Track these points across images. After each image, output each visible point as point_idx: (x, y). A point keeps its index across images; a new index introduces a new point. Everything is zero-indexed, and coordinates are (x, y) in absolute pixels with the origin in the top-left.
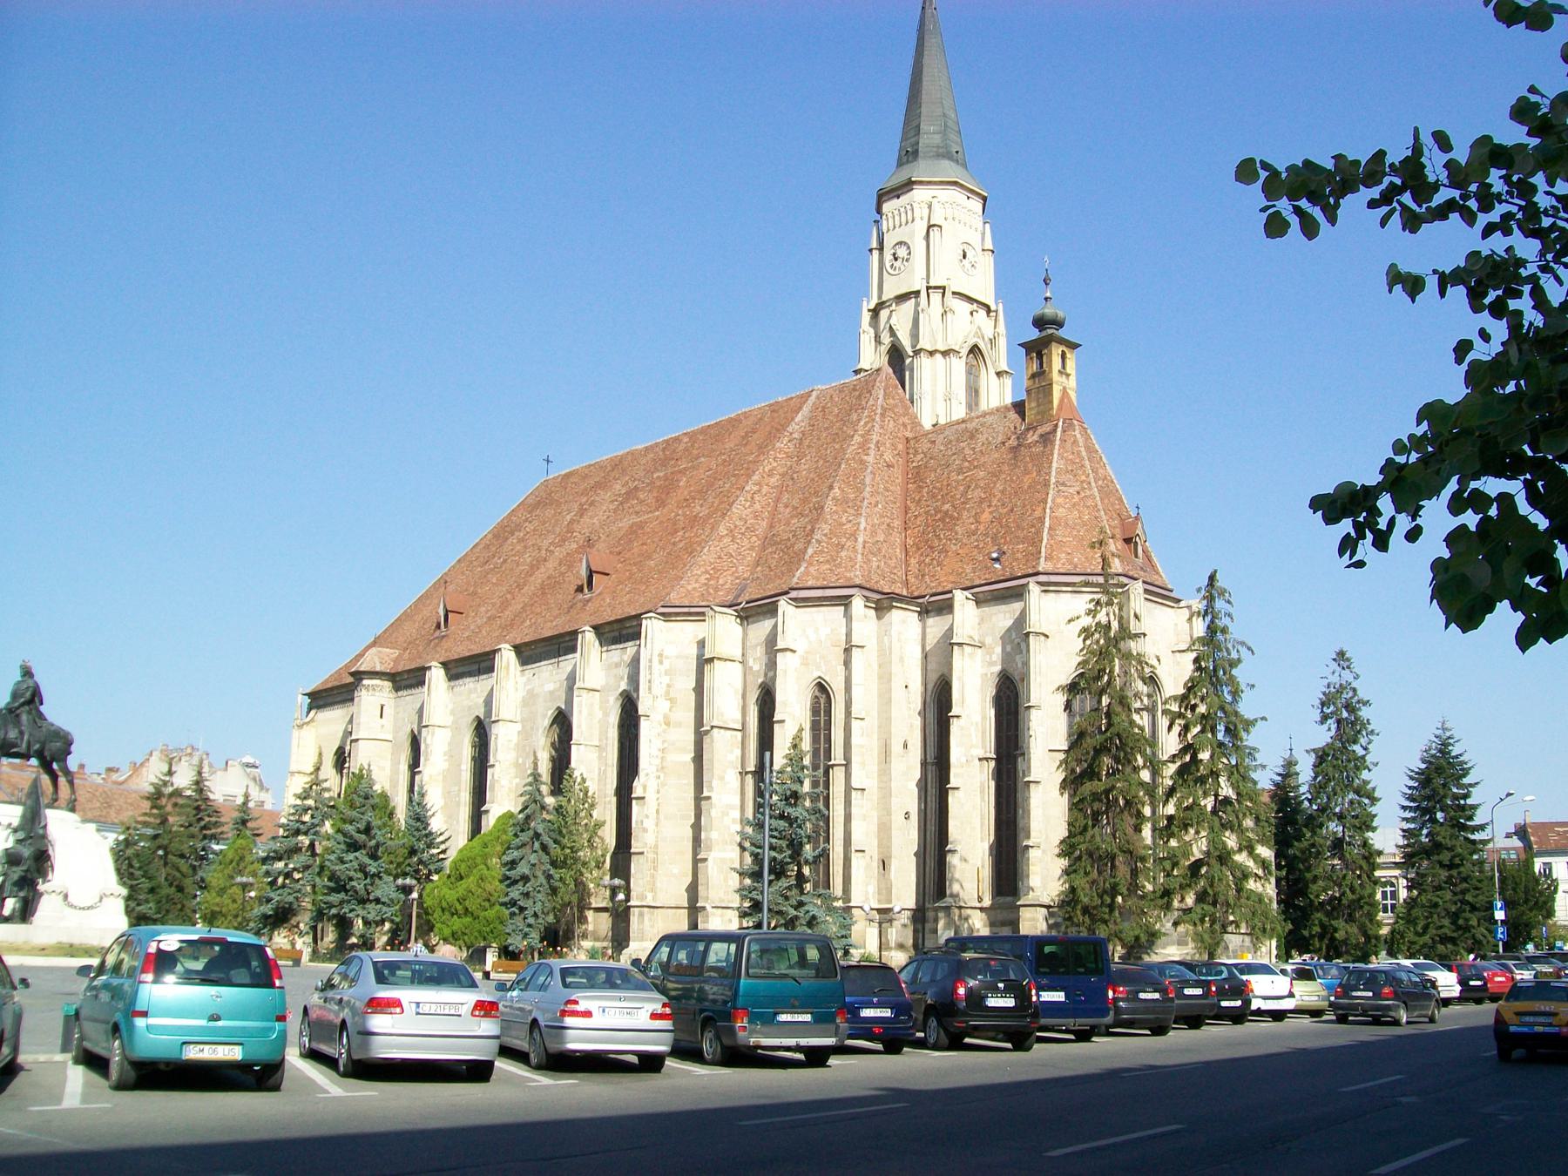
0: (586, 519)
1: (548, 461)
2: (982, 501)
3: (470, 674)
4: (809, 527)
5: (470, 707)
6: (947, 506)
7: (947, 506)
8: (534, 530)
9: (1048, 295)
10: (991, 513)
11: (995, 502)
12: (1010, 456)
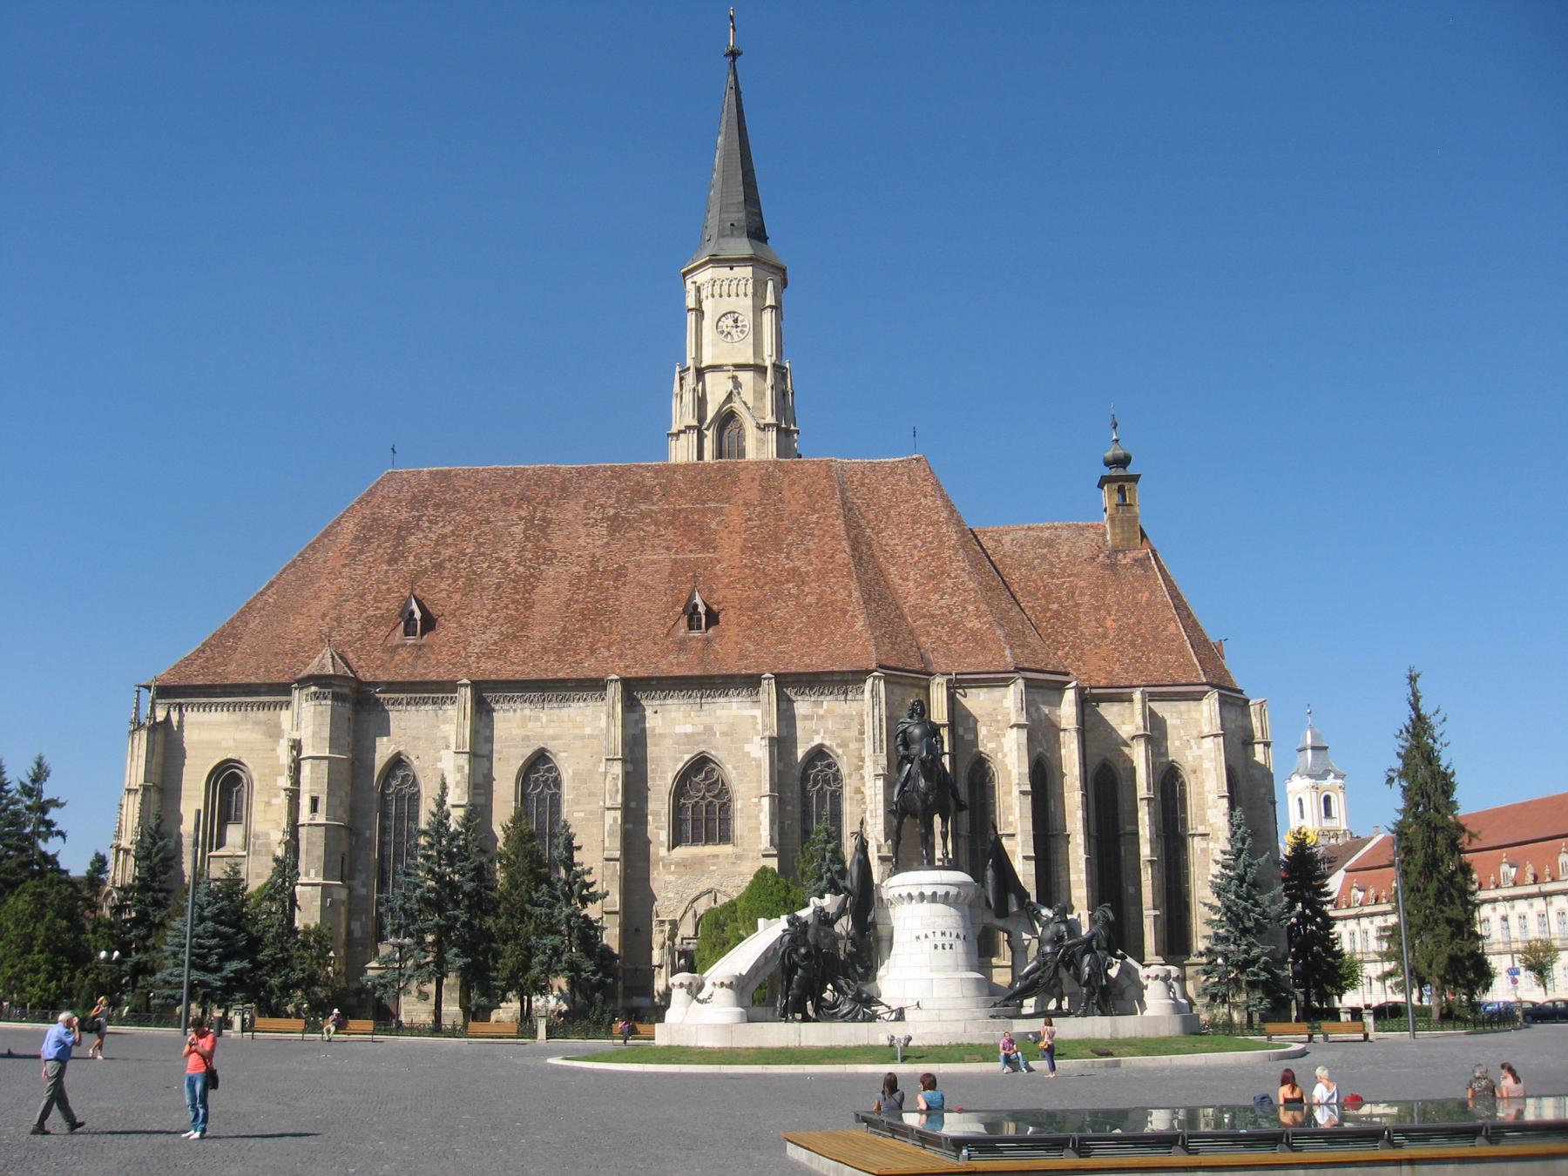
0: (558, 540)
1: (394, 452)
2: (1097, 609)
4: (971, 608)
5: (526, 738)
6: (1055, 606)
7: (1055, 606)
8: (453, 533)
9: (1114, 437)
10: (1113, 620)
12: (1108, 572)
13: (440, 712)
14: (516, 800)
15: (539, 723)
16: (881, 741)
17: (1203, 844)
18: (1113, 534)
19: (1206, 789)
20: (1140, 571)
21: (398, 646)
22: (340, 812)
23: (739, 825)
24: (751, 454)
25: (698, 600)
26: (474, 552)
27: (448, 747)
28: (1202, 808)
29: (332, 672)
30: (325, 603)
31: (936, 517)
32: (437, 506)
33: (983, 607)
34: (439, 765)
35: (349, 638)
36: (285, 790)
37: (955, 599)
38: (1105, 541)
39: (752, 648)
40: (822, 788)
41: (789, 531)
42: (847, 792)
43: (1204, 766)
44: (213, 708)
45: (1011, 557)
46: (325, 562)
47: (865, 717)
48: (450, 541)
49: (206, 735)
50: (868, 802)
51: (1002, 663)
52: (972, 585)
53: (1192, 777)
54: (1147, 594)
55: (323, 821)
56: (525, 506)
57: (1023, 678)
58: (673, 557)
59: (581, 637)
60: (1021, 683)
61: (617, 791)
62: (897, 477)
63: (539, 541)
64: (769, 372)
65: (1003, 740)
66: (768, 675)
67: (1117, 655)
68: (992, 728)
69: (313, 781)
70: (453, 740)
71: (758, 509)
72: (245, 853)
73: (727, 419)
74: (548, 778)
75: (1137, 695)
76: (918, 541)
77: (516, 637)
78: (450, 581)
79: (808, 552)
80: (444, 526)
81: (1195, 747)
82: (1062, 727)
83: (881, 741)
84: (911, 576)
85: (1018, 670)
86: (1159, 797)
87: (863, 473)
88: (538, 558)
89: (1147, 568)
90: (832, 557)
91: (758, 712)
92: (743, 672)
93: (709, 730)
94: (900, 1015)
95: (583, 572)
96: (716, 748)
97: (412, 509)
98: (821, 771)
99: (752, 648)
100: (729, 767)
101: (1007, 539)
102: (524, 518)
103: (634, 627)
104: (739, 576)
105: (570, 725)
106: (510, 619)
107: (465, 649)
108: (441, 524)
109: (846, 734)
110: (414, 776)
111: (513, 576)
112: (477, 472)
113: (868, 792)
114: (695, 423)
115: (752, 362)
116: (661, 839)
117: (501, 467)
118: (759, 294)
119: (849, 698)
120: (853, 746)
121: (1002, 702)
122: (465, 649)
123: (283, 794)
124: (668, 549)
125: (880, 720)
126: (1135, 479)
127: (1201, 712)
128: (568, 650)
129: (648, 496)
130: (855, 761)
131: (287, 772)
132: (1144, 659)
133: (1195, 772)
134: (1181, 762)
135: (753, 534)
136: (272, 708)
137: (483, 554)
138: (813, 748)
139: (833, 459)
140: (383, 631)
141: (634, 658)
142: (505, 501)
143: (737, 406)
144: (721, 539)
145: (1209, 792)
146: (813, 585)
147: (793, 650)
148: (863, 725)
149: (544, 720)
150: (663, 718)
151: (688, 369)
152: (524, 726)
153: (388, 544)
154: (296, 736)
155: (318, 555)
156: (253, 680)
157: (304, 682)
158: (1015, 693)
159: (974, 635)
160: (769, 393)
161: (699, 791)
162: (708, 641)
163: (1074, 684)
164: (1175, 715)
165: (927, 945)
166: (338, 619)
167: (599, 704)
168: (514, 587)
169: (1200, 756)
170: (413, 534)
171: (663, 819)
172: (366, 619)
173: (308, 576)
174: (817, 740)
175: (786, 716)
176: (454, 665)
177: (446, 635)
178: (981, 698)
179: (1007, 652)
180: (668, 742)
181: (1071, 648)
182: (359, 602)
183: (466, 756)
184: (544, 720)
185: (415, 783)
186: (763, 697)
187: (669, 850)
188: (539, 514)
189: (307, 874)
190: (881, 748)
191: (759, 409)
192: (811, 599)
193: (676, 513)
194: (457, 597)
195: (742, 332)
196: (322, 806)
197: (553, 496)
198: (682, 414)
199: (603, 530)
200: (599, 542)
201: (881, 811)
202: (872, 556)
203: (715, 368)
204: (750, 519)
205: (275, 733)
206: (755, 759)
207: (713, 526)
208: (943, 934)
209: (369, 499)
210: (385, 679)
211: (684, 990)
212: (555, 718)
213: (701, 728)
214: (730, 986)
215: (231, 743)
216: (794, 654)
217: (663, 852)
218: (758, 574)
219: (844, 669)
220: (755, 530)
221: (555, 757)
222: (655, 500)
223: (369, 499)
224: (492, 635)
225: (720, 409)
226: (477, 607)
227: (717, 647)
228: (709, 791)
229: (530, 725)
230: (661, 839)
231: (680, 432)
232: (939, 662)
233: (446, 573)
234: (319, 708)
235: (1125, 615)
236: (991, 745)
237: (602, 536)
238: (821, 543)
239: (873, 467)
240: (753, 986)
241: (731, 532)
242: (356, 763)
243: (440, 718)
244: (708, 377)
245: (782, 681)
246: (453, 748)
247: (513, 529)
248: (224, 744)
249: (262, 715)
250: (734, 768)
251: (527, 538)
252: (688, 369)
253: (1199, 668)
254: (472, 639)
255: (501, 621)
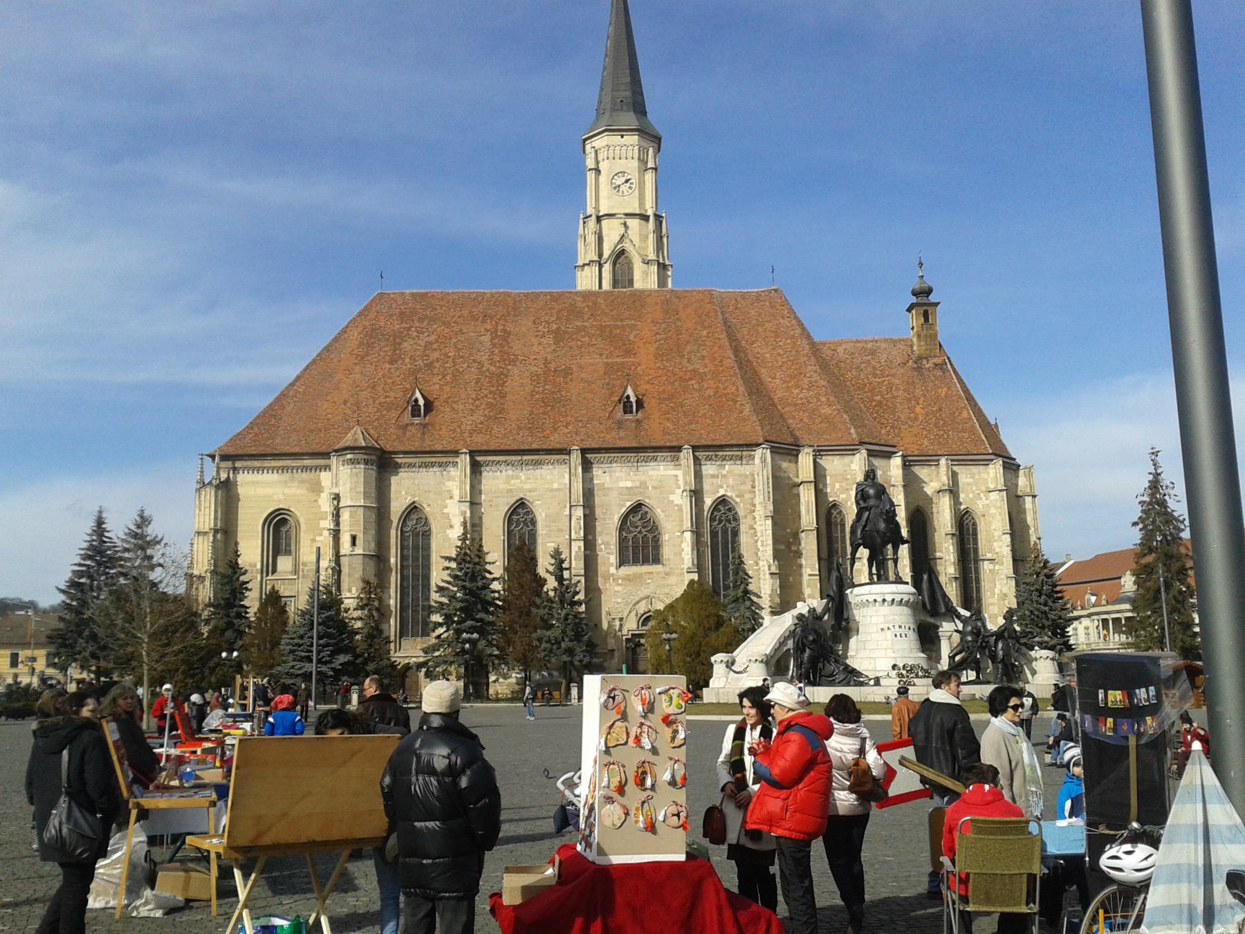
0: (517, 347)
3: (507, 463)
4: (823, 399)
6: (878, 398)
9: (920, 274)
11: (921, 402)
13: (445, 473)
14: (504, 535)
15: (519, 481)
16: (769, 492)
17: (991, 567)
18: (919, 346)
19: (992, 528)
20: (939, 373)
21: (407, 425)
22: (373, 545)
23: (667, 552)
24: (638, 284)
25: (630, 392)
26: (455, 355)
27: (451, 497)
28: (990, 540)
29: (364, 444)
30: (344, 392)
31: (792, 333)
32: (421, 320)
33: (832, 398)
34: (446, 511)
35: (368, 418)
36: (329, 530)
37: (811, 393)
38: (913, 351)
39: (671, 427)
40: (725, 525)
41: (688, 342)
42: (743, 528)
43: (991, 512)
44: (265, 471)
45: (844, 362)
46: (339, 361)
47: (756, 476)
48: (435, 346)
49: (260, 491)
50: (759, 535)
51: (850, 439)
52: (823, 383)
53: (982, 519)
54: (945, 389)
55: (361, 552)
56: (489, 321)
57: (867, 450)
58: (605, 361)
59: (545, 419)
60: (864, 452)
61: (580, 529)
62: (761, 303)
63: (503, 347)
64: (652, 219)
65: (851, 492)
66: (686, 446)
67: (925, 433)
68: (843, 484)
69: (350, 523)
70: (456, 493)
71: (663, 325)
72: (295, 577)
73: (620, 255)
74: (526, 519)
75: (943, 461)
76: (779, 351)
77: (496, 418)
78: (440, 377)
79: (703, 358)
80: (428, 335)
81: (984, 498)
82: (892, 483)
83: (769, 492)
84: (778, 377)
85: (862, 443)
86: (958, 533)
87: (736, 300)
88: (505, 360)
89: (944, 370)
90: (721, 361)
91: (679, 473)
92: (668, 444)
93: (643, 485)
94: (877, 682)
95: (540, 371)
96: (649, 498)
97: (402, 323)
98: (725, 513)
99: (671, 427)
100: (659, 510)
101: (840, 350)
102: (489, 330)
103: (584, 412)
104: (655, 375)
105: (542, 482)
106: (490, 405)
107: (459, 427)
108: (426, 334)
109: (742, 487)
110: (426, 519)
111: (488, 374)
112: (448, 294)
113: (758, 528)
114: (596, 258)
115: (638, 212)
116: (611, 561)
117: (466, 291)
118: (643, 161)
119: (744, 462)
120: (748, 496)
121: (850, 466)
122: (459, 427)
123: (326, 533)
124: (601, 354)
125: (768, 478)
126: (937, 304)
127: (988, 473)
128: (537, 428)
129: (579, 314)
130: (749, 506)
131: (330, 517)
132: (945, 436)
133: (984, 516)
134: (974, 509)
135: (662, 344)
136: (313, 471)
137: (462, 357)
138: (719, 498)
139: (714, 289)
140: (394, 414)
141: (587, 434)
142: (474, 318)
143: (627, 245)
144: (639, 347)
145: (995, 530)
146: (710, 382)
147: (701, 429)
148: (754, 481)
149: (523, 478)
150: (610, 476)
151: (590, 216)
152: (508, 482)
153: (387, 349)
154: (336, 491)
155: (332, 356)
156: (297, 450)
157: (341, 451)
158: (860, 459)
159: (826, 419)
160: (651, 236)
161: (637, 527)
162: (638, 422)
163: (900, 453)
164: (969, 476)
165: (889, 634)
166: (357, 404)
167: (563, 466)
168: (490, 382)
169: (988, 505)
170: (406, 341)
171: (612, 547)
172: (380, 403)
173: (327, 372)
174: (721, 492)
175: (698, 476)
176: (453, 438)
177: (443, 417)
178: (835, 463)
179: (853, 431)
180: (614, 494)
181: (892, 427)
182: (371, 392)
183: (468, 504)
184: (523, 478)
185: (427, 523)
186: (683, 462)
187: (617, 569)
188: (500, 328)
189: (350, 591)
190: (769, 498)
191: (644, 248)
192: (710, 392)
193: (602, 328)
194: (447, 388)
195: (630, 188)
196: (359, 541)
197: (509, 314)
198: (586, 253)
199: (549, 340)
200: (548, 350)
201: (770, 542)
202: (748, 361)
203: (610, 215)
204: (657, 334)
205: (317, 489)
206: (677, 505)
207: (631, 338)
208: (900, 627)
209: (366, 313)
210: (402, 449)
211: (724, 665)
212: (531, 477)
213: (638, 484)
214: (762, 662)
215: (282, 497)
216: (703, 432)
217: (613, 570)
218: (668, 374)
219: (740, 443)
220: (662, 342)
221: (532, 504)
222: (585, 318)
223: (366, 313)
224: (478, 417)
225: (615, 247)
226: (463, 396)
227: (646, 427)
228: (644, 527)
229: (512, 482)
230: (611, 561)
231: (584, 265)
232: (804, 437)
233: (436, 371)
234: (354, 470)
235: (930, 405)
236: (843, 496)
237: (550, 345)
238: (712, 351)
239: (743, 295)
240: (774, 661)
241: (644, 343)
242: (382, 510)
243: (445, 477)
244: (604, 223)
245: (695, 448)
246: (457, 498)
247: (482, 338)
248: (276, 498)
249: (305, 475)
250: (662, 511)
251: (494, 345)
252: (590, 216)
253: (986, 443)
254: (463, 419)
255: (483, 406)
